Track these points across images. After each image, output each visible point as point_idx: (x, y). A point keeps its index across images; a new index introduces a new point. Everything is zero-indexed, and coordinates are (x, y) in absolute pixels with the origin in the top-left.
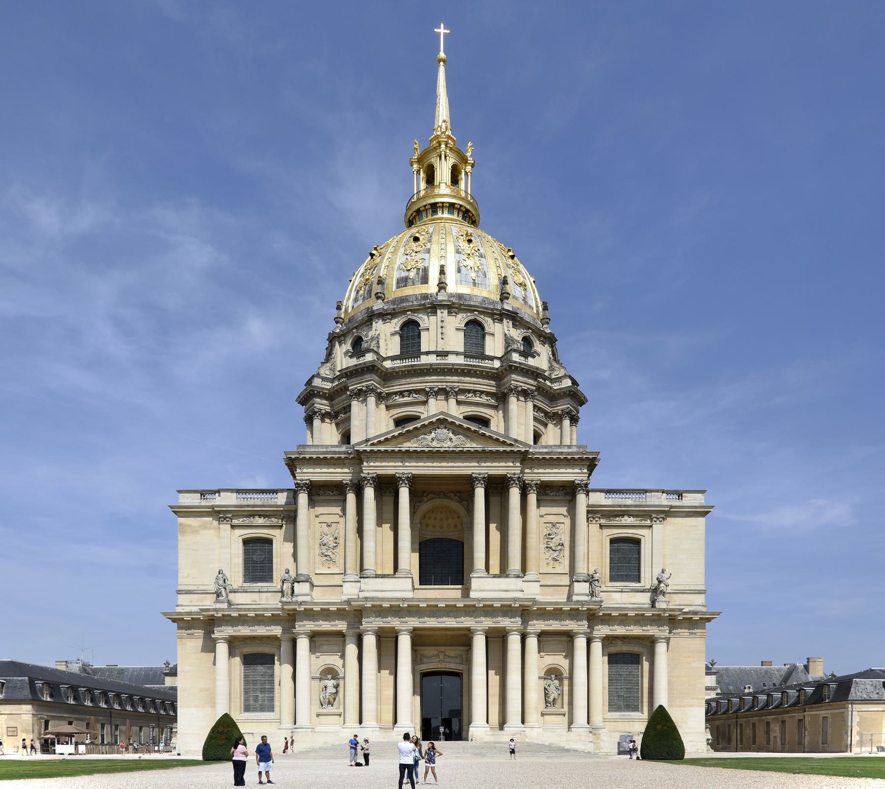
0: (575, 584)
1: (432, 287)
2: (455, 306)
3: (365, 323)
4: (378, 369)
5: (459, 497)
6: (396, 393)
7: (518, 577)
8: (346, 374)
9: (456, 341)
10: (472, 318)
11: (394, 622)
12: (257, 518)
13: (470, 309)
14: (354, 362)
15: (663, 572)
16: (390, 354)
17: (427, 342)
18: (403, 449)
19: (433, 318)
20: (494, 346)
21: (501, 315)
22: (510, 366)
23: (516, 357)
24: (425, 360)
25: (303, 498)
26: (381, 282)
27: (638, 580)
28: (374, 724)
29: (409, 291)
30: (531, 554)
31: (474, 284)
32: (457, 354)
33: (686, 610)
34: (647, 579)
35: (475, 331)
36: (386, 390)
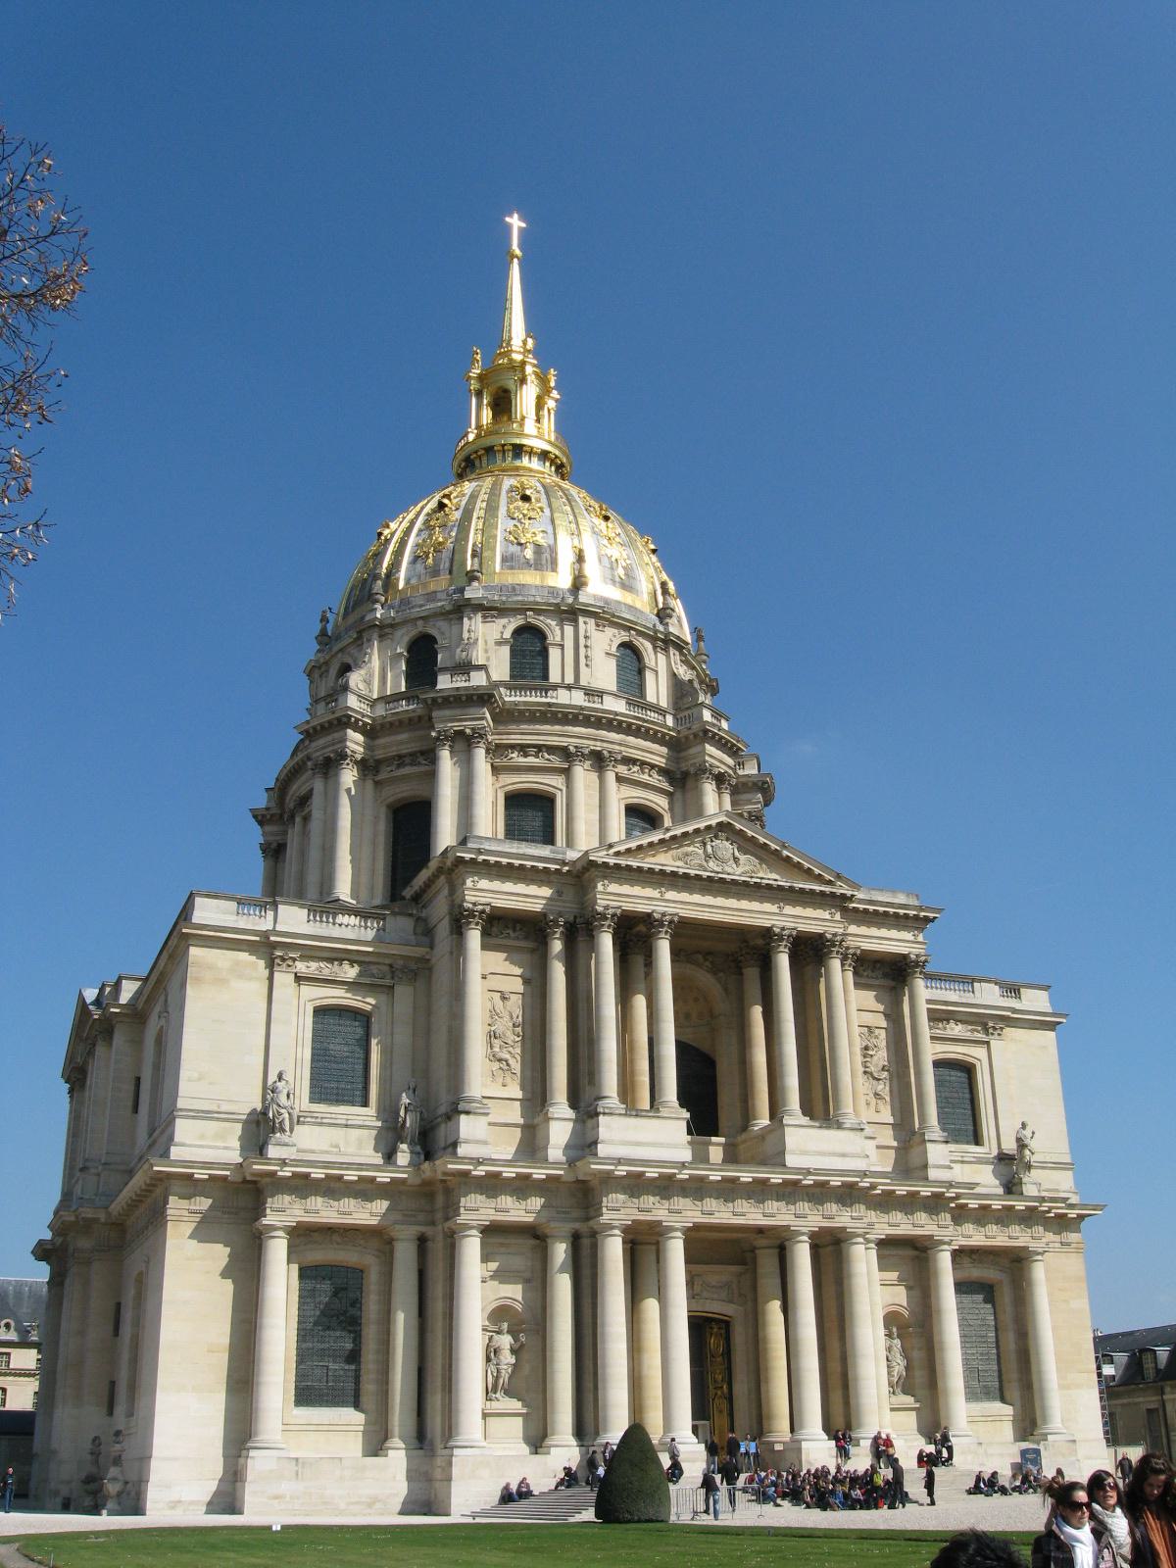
0: (929, 1145)
1: (562, 580)
2: (604, 616)
3: (442, 614)
4: (496, 701)
5: (712, 962)
6: (513, 747)
8: (434, 700)
9: (604, 673)
10: (627, 639)
11: (657, 1210)
12: (346, 965)
15: (1024, 1126)
17: (557, 666)
18: (668, 869)
19: (569, 630)
20: (657, 690)
22: (706, 731)
27: (977, 1139)
35: (631, 660)
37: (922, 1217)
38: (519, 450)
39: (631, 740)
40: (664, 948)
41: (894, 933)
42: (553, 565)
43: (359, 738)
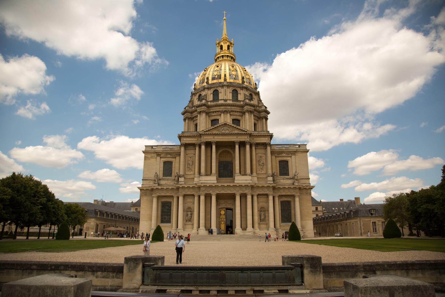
1: (222, 80)
7: (250, 175)
9: (230, 96)
13: (233, 86)
14: (199, 103)
16: (210, 100)
17: (221, 96)
19: (222, 89)
20: (241, 97)
21: (243, 88)
23: (247, 101)
24: (221, 102)
25: (183, 149)
26: (208, 78)
28: (204, 228)
29: (215, 81)
30: (254, 167)
31: (235, 79)
32: (230, 100)
33: (304, 185)
34: (291, 175)
36: (208, 111)
37: (266, 190)
38: (223, 56)
39: (233, 108)
40: (214, 147)
41: (263, 139)
42: (220, 78)
43: (190, 114)
